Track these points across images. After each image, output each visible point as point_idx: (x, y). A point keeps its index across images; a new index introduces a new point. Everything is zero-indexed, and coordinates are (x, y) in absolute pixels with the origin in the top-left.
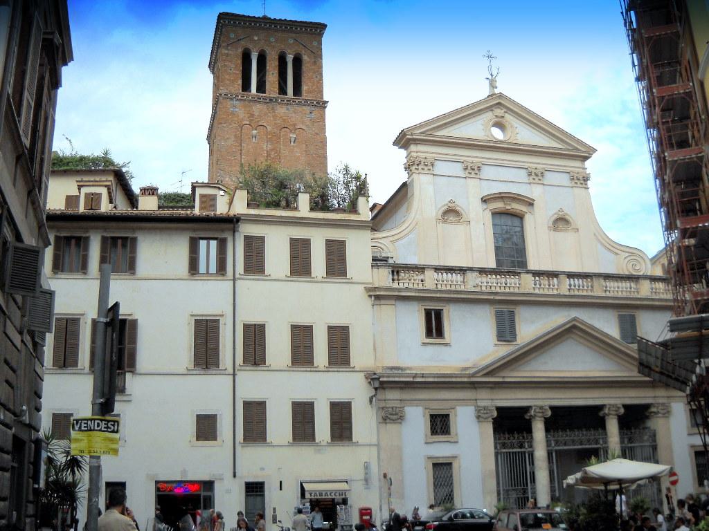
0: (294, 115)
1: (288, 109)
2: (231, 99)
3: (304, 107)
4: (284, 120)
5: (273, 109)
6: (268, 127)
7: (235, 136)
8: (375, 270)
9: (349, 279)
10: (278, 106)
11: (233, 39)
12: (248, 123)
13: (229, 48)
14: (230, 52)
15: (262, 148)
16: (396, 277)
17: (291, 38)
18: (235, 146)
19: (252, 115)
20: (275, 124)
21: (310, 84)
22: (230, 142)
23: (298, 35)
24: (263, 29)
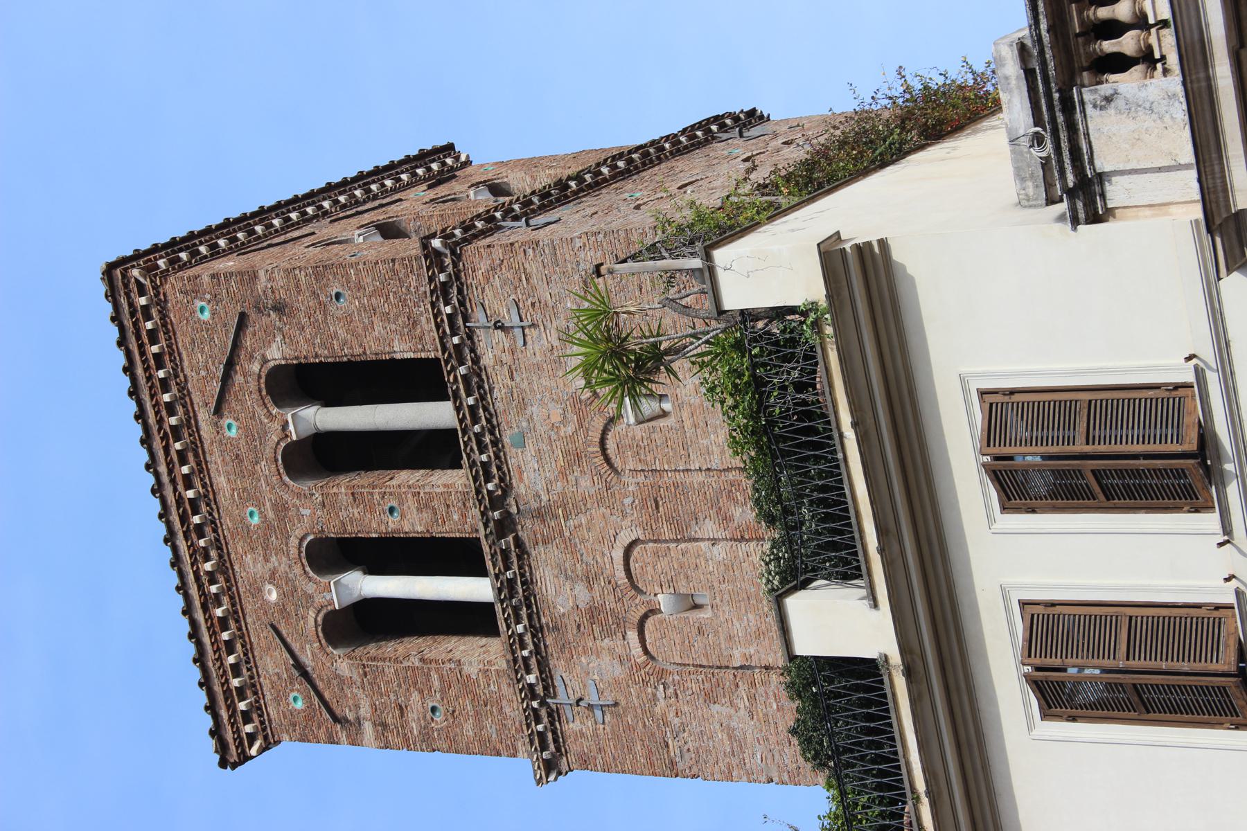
0: (535, 410)
1: (521, 443)
2: (555, 716)
3: (487, 360)
4: (574, 458)
5: (540, 514)
6: (625, 538)
7: (710, 698)
8: (1116, 193)
9: (1199, 373)
10: (520, 488)
11: (307, 698)
12: (633, 636)
13: (351, 716)
14: (365, 711)
15: (729, 567)
16: (1127, 43)
17: (218, 428)
18: (752, 698)
19: (593, 613)
20: (600, 501)
21: (378, 328)
22: (741, 721)
23: (197, 398)
24: (225, 568)
